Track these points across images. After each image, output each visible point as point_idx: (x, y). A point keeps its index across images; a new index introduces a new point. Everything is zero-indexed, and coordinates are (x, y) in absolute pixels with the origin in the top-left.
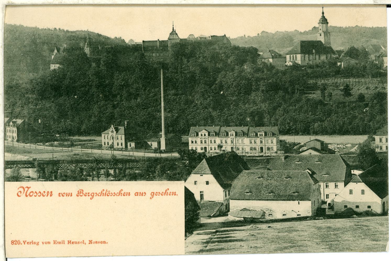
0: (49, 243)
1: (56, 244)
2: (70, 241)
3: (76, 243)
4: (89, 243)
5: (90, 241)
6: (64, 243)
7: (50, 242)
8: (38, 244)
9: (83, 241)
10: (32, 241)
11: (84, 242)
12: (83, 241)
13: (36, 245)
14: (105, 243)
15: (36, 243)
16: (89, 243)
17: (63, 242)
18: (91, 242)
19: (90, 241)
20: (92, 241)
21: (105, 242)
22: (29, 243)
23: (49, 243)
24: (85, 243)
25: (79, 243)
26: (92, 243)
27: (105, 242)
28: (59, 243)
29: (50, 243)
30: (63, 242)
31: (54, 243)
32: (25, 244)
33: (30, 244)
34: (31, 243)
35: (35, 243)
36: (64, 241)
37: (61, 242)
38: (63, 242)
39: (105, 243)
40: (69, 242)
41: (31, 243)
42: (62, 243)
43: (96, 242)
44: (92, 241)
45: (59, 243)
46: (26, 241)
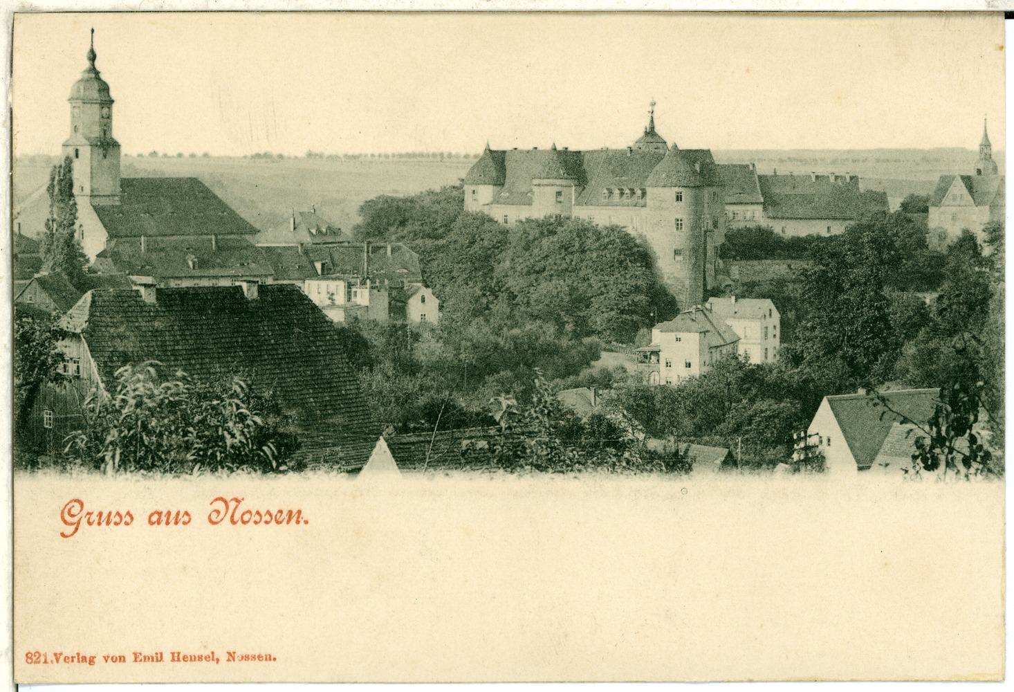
0: (122, 659)
1: (141, 661)
2: (179, 653)
3: (193, 659)
4: (229, 660)
5: (229, 653)
7: (124, 658)
9: (213, 653)
10: (78, 654)
11: (215, 657)
12: (213, 653)
13: (86, 665)
14: (270, 660)
15: (88, 660)
16: (229, 660)
17: (159, 655)
18: (231, 656)
19: (229, 653)
20: (234, 653)
21: (269, 658)
22: (70, 659)
23: (122, 659)
24: (218, 660)
25: (200, 658)
26: (234, 660)
27: (269, 658)
28: (146, 659)
29: (124, 661)
30: (159, 658)
31: (136, 661)
32: (57, 661)
33: (73, 661)
34: (76, 660)
35: (84, 659)
36: (161, 654)
37: (153, 658)
38: (159, 658)
39: (270, 660)
40: (176, 657)
41: (76, 660)
42: (155, 659)
44: (234, 653)
45: (146, 659)
46: (61, 654)
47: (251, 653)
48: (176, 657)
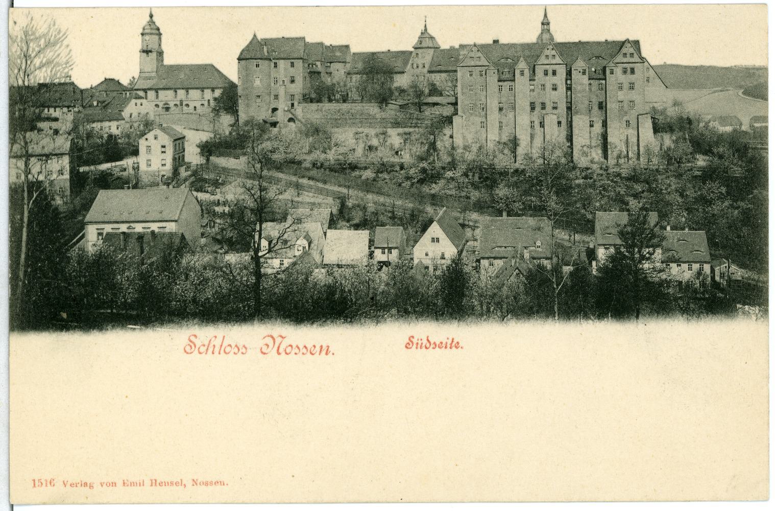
0: (114, 484)
6: (143, 485)
8: (91, 487)
9: (181, 480)
11: (183, 483)
12: (181, 480)
14: (224, 484)
16: (193, 485)
18: (195, 482)
23: (114, 484)
24: (185, 485)
25: (172, 483)
26: (196, 484)
28: (133, 484)
30: (142, 484)
33: (76, 486)
35: (86, 484)
38: (142, 484)
40: (154, 483)
43: (206, 484)
45: (133, 484)
47: (209, 480)
48: (154, 483)
